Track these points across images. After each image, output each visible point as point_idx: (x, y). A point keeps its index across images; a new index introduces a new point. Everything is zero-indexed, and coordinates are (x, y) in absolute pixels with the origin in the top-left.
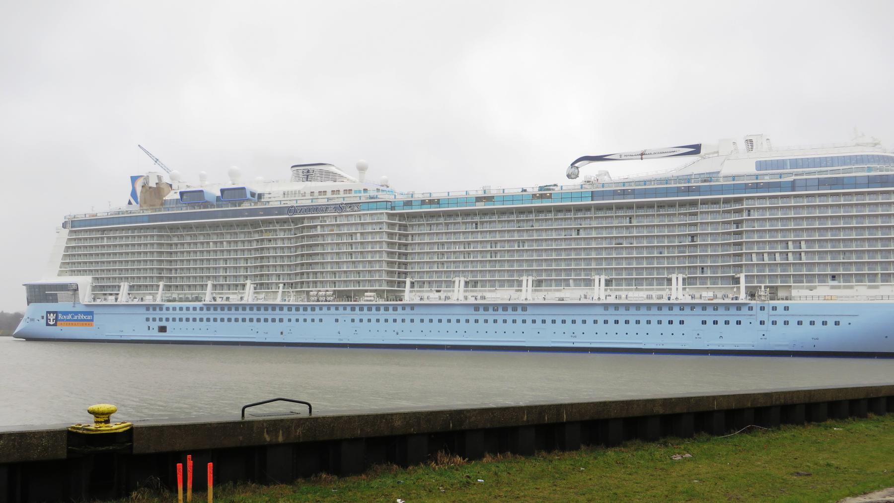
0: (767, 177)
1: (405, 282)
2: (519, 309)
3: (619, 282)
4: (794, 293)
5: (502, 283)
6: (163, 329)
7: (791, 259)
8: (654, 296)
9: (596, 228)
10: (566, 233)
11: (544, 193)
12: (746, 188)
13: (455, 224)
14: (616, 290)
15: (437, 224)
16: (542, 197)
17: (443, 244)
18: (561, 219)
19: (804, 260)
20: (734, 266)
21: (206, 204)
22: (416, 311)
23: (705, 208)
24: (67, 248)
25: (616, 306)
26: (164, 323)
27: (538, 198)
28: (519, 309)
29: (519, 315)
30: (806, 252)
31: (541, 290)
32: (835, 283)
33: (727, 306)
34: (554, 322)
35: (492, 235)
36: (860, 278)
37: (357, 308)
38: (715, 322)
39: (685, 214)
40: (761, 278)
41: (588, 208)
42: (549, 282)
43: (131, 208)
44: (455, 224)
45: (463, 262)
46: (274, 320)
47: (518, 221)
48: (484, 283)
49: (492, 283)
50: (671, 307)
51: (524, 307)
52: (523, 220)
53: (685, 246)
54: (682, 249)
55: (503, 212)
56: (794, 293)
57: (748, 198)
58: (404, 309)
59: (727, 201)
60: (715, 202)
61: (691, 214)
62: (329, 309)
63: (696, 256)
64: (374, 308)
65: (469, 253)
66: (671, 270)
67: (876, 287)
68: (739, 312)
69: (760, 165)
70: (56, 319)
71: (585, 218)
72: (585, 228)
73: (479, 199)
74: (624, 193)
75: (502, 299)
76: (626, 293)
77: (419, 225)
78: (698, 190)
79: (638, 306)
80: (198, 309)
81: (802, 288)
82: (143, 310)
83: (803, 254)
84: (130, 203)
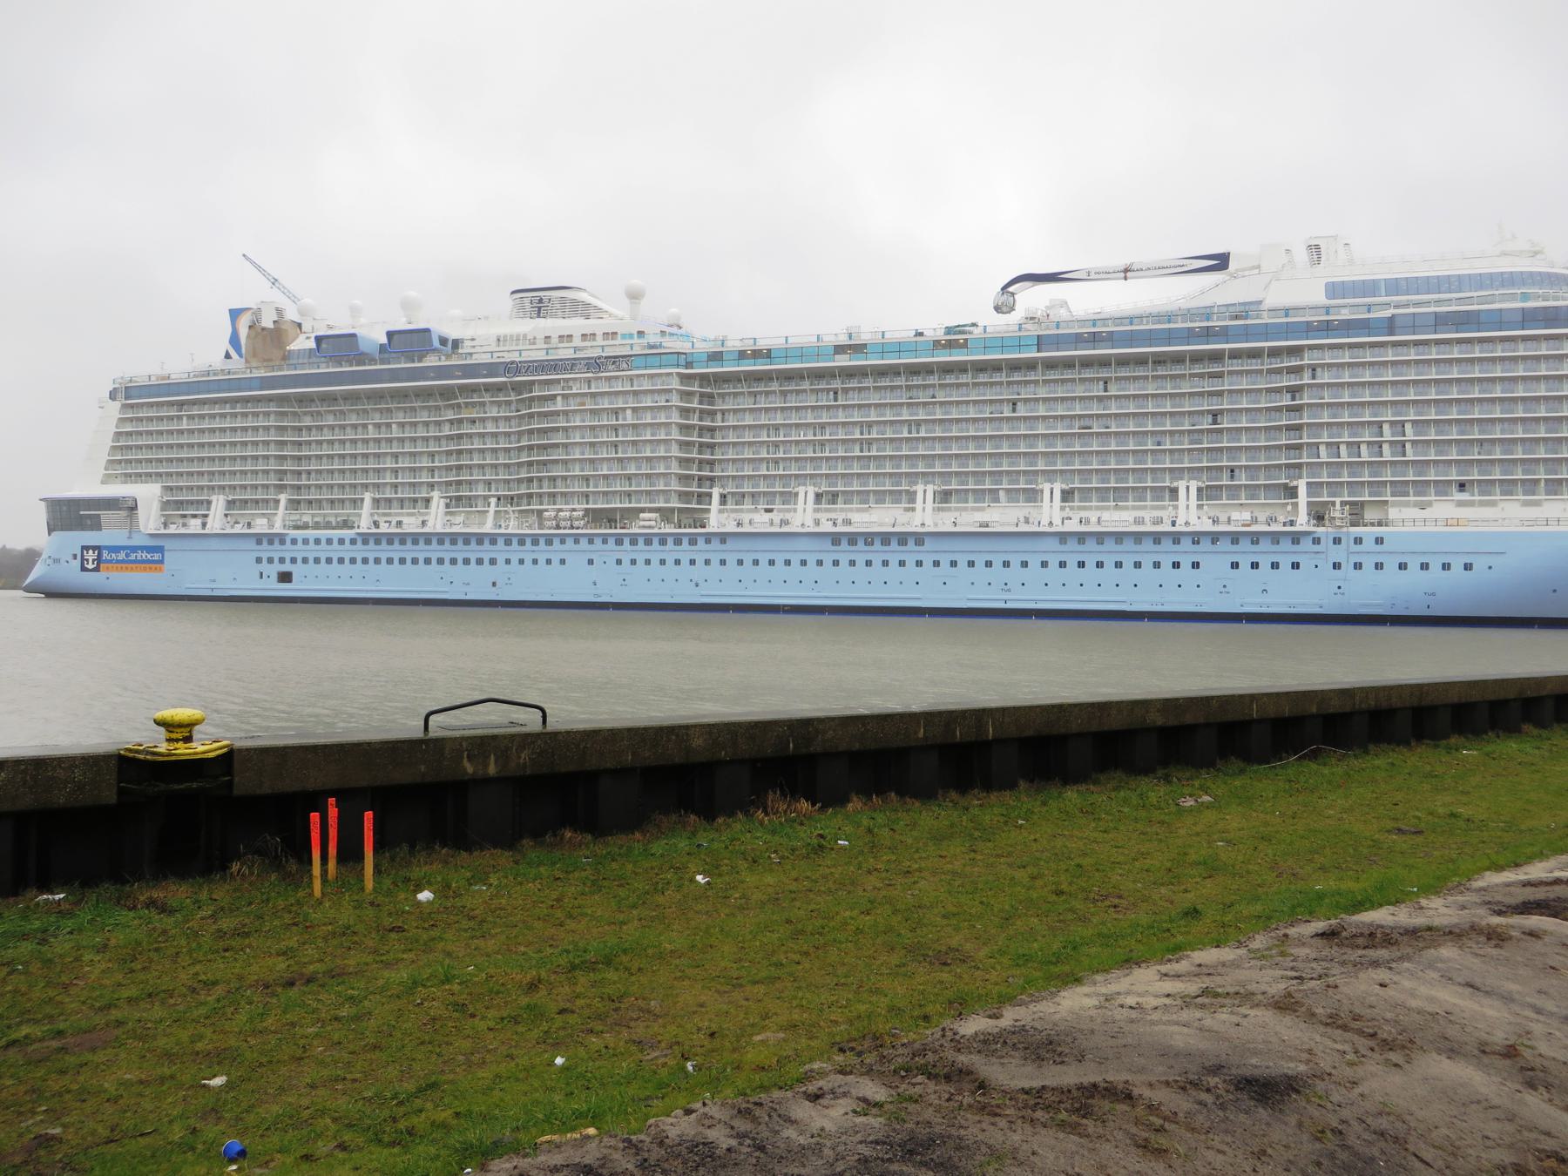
0: (1344, 311)
1: (710, 495)
2: (911, 542)
3: (1086, 494)
4: (1393, 513)
5: (880, 496)
6: (285, 577)
7: (1387, 454)
8: (1147, 520)
9: (1045, 400)
10: (993, 408)
11: (955, 338)
12: (1309, 329)
13: (798, 392)
14: (1080, 508)
15: (767, 393)
16: (951, 345)
17: (777, 428)
18: (985, 384)
19: (1410, 456)
20: (1288, 466)
21: (362, 358)
22: (729, 545)
23: (1236, 365)
24: (118, 434)
25: (1081, 537)
26: (287, 567)
27: (944, 347)
28: (911, 542)
29: (911, 553)
30: (1414, 442)
31: (949, 509)
32: (1464, 496)
33: (1275, 537)
34: (971, 564)
35: (863, 411)
36: (1508, 487)
37: (626, 541)
38: (1255, 565)
39: (1201, 376)
40: (1334, 487)
41: (1031, 365)
42: (963, 495)
43: (230, 365)
44: (798, 392)
45: (812, 459)
46: (480, 562)
47: (909, 388)
48: (849, 496)
49: (864, 496)
50: (1176, 538)
51: (919, 538)
52: (918, 387)
53: (1201, 431)
54: (1196, 436)
55: (881, 372)
56: (1393, 513)
57: (1311, 348)
58: (708, 541)
59: (1274, 353)
60: (1255, 354)
61: (1212, 376)
62: (577, 541)
63: (1220, 449)
64: (656, 541)
65: (822, 444)
66: (1177, 473)
67: (1537, 503)
68: (1296, 548)
69: (1334, 290)
70: (99, 560)
71: (1027, 383)
72: (1026, 400)
73: (839, 349)
74: (1095, 339)
75: (881, 525)
76: (1098, 513)
77: (736, 395)
78: (1224, 334)
79: (1119, 537)
80: (347, 542)
81: (1407, 504)
82: (252, 544)
83: (1408, 446)
84: (228, 356)
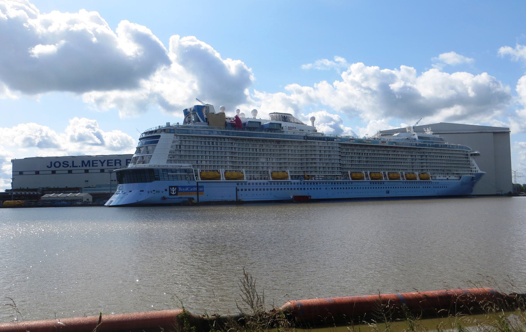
70: (177, 191)
